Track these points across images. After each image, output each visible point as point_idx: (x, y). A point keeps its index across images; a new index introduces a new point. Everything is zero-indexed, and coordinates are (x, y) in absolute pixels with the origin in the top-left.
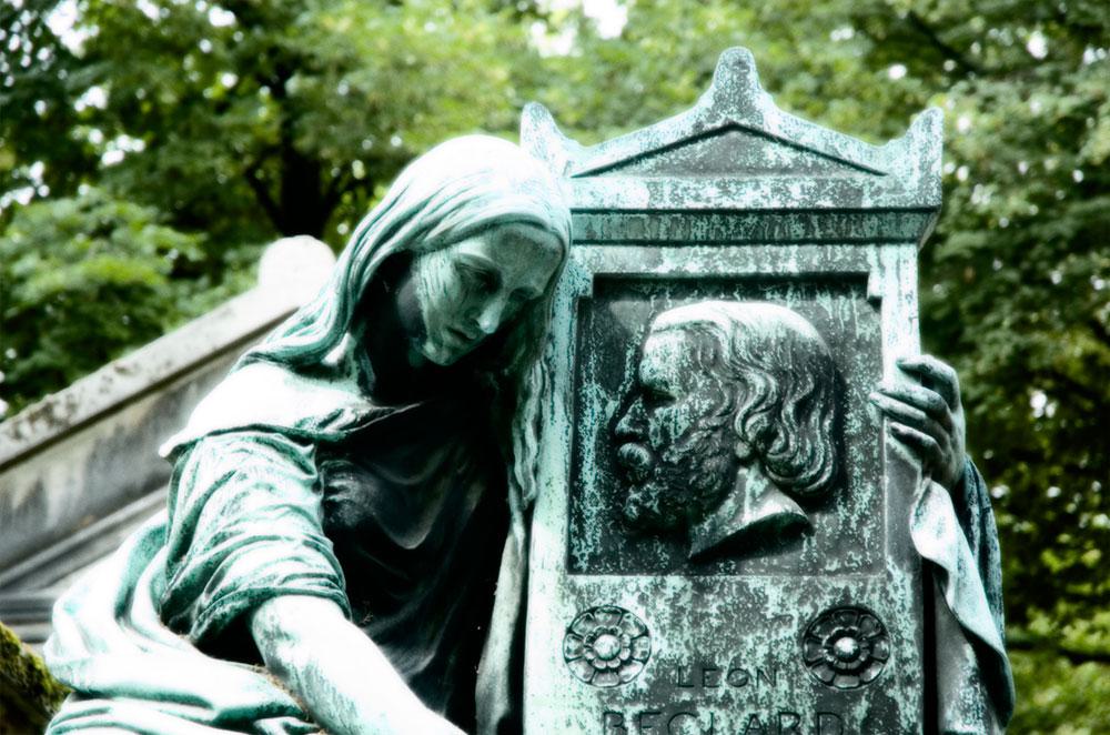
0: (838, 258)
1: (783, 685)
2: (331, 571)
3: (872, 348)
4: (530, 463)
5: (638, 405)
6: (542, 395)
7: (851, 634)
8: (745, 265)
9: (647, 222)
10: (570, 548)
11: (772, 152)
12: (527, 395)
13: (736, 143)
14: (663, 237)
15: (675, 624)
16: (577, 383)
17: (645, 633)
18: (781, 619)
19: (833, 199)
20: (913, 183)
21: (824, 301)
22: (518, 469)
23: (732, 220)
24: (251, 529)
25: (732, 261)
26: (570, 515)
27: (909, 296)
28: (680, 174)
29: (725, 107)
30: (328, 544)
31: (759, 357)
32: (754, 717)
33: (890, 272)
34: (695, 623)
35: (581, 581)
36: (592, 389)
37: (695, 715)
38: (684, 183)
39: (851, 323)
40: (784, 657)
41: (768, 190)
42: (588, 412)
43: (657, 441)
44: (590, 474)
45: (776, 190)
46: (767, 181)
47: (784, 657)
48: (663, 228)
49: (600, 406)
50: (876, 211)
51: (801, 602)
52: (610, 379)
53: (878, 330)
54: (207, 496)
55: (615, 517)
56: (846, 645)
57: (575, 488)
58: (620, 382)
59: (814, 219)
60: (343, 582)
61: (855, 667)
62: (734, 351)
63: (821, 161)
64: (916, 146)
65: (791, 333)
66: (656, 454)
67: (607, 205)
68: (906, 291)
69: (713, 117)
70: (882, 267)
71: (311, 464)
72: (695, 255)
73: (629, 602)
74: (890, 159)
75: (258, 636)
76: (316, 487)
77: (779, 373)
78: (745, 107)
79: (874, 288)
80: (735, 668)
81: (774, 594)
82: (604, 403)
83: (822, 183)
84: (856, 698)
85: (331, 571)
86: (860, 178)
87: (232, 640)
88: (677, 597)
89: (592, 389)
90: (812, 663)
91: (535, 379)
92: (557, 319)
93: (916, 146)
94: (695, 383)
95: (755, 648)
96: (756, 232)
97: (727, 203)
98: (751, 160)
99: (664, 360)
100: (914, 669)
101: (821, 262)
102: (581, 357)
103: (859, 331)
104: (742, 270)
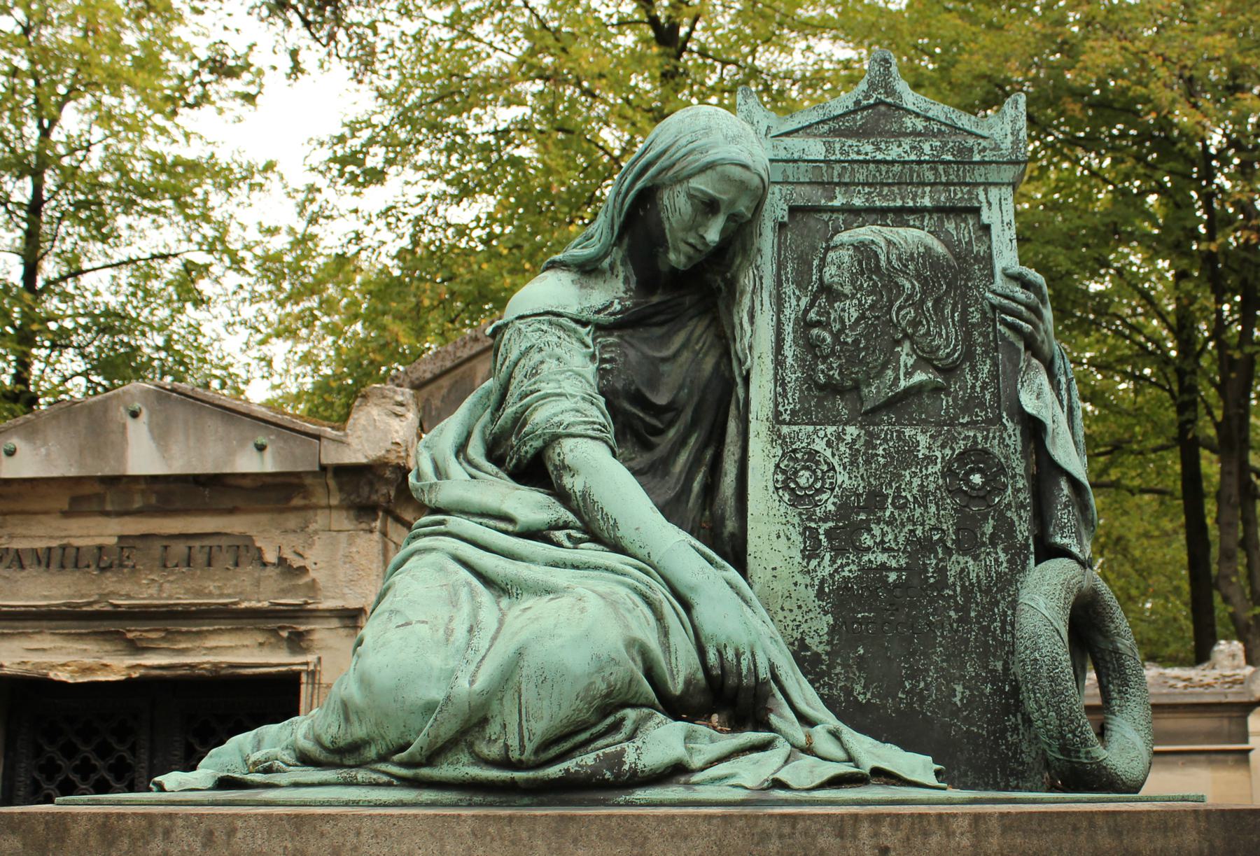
0: (959, 195)
2: (602, 420)
3: (988, 260)
4: (746, 341)
5: (823, 300)
6: (753, 292)
7: (980, 471)
8: (894, 200)
9: (824, 169)
10: (776, 405)
11: (909, 122)
12: (742, 293)
13: (884, 114)
14: (836, 180)
15: (853, 462)
16: (779, 283)
17: (833, 469)
18: (931, 460)
19: (954, 155)
21: (950, 226)
22: (738, 345)
23: (884, 168)
24: (547, 388)
25: (885, 197)
26: (776, 381)
27: (1009, 224)
28: (847, 137)
29: (875, 90)
30: (601, 401)
31: (906, 266)
32: (913, 531)
33: (995, 207)
35: (785, 430)
36: (789, 289)
37: (869, 530)
38: (850, 142)
39: (969, 243)
41: (907, 148)
42: (787, 305)
43: (836, 327)
44: (789, 351)
45: (913, 148)
46: (907, 143)
47: (932, 487)
48: (836, 173)
49: (795, 303)
50: (982, 163)
51: (943, 446)
52: (801, 284)
53: (990, 247)
54: (516, 364)
55: (809, 380)
56: (977, 479)
57: (779, 362)
58: (809, 284)
59: (941, 168)
60: (612, 429)
61: (983, 496)
62: (889, 262)
63: (943, 128)
64: (1008, 119)
65: (928, 249)
66: (836, 336)
67: (796, 156)
68: (1006, 220)
69: (867, 97)
70: (989, 204)
71: (589, 340)
72: (859, 192)
73: (819, 445)
74: (991, 127)
75: (551, 468)
76: (593, 357)
77: (918, 276)
78: (891, 91)
79: (985, 218)
80: (897, 496)
81: (923, 440)
82: (799, 299)
83: (945, 144)
84: (985, 519)
85: (602, 420)
86: (971, 141)
87: (535, 471)
88: (854, 441)
89: (789, 289)
90: (953, 492)
91: (747, 281)
92: (764, 237)
93: (1008, 119)
94: (862, 284)
95: (912, 482)
96: (900, 177)
97: (880, 156)
98: (895, 127)
99: (839, 267)
101: (947, 199)
102: (780, 266)
103: (975, 249)
104: (892, 204)
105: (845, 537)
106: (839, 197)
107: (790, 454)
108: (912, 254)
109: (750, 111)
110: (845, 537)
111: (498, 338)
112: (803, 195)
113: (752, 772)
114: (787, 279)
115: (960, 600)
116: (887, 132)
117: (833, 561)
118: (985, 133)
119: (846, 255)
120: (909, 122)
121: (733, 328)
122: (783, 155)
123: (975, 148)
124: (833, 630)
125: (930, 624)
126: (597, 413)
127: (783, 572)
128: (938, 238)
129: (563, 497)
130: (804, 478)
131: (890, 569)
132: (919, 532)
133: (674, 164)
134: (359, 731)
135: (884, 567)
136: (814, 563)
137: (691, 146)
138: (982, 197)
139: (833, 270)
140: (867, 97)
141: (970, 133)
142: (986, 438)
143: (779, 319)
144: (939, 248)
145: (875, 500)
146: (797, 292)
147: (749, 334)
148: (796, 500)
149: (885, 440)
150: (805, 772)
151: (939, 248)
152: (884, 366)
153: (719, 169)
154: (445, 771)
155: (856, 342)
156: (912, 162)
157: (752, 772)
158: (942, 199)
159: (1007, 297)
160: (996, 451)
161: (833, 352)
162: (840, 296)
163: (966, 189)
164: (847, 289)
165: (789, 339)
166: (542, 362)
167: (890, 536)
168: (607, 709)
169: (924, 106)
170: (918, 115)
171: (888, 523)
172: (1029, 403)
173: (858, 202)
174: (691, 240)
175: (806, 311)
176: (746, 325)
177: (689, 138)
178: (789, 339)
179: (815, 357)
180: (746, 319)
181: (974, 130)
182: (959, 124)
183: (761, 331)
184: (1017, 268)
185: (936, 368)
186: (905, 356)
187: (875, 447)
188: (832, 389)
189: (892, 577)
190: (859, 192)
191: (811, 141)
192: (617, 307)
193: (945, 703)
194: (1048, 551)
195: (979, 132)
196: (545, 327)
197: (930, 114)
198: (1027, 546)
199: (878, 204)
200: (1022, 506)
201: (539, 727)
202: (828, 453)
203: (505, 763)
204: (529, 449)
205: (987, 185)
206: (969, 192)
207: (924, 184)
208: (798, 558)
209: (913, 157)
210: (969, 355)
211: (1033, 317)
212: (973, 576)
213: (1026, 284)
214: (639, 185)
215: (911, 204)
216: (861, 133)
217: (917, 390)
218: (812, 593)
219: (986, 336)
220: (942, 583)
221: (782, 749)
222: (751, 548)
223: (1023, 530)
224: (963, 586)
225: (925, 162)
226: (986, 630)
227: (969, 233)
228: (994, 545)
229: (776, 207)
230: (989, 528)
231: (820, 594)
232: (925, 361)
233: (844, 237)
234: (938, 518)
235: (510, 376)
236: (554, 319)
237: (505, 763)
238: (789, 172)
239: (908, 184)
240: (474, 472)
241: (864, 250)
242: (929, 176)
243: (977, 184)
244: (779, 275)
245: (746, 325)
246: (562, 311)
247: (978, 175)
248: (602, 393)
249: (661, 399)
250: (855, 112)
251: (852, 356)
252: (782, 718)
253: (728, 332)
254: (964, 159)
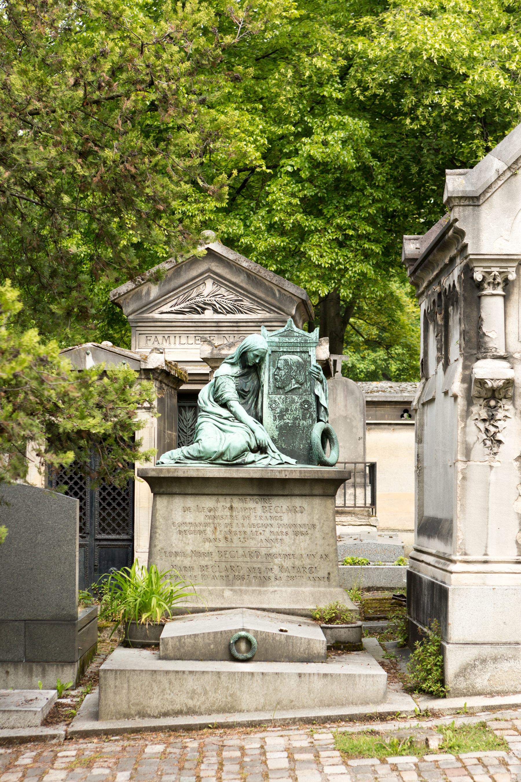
3: (310, 362)
44: (271, 380)
49: (272, 370)
52: (274, 366)
55: (275, 386)
61: (307, 409)
87: (225, 405)
91: (263, 367)
95: (294, 406)
105: (281, 417)
107: (271, 401)
110: (281, 417)
112: (274, 348)
113: (265, 462)
119: (282, 361)
120: (295, 334)
126: (236, 396)
129: (231, 411)
130: (274, 405)
134: (202, 455)
144: (301, 360)
148: (272, 410)
150: (274, 462)
151: (301, 360)
154: (217, 462)
157: (265, 462)
168: (243, 452)
172: (317, 392)
183: (266, 376)
186: (293, 381)
188: (279, 388)
193: (299, 448)
194: (319, 420)
201: (233, 454)
203: (227, 461)
204: (224, 402)
210: (306, 381)
213: (317, 368)
216: (286, 336)
217: (296, 388)
221: (270, 458)
223: (315, 416)
229: (269, 352)
232: (297, 382)
233: (281, 358)
234: (299, 413)
237: (227, 461)
241: (286, 361)
249: (247, 390)
251: (283, 382)
252: (269, 451)
254: (306, 342)
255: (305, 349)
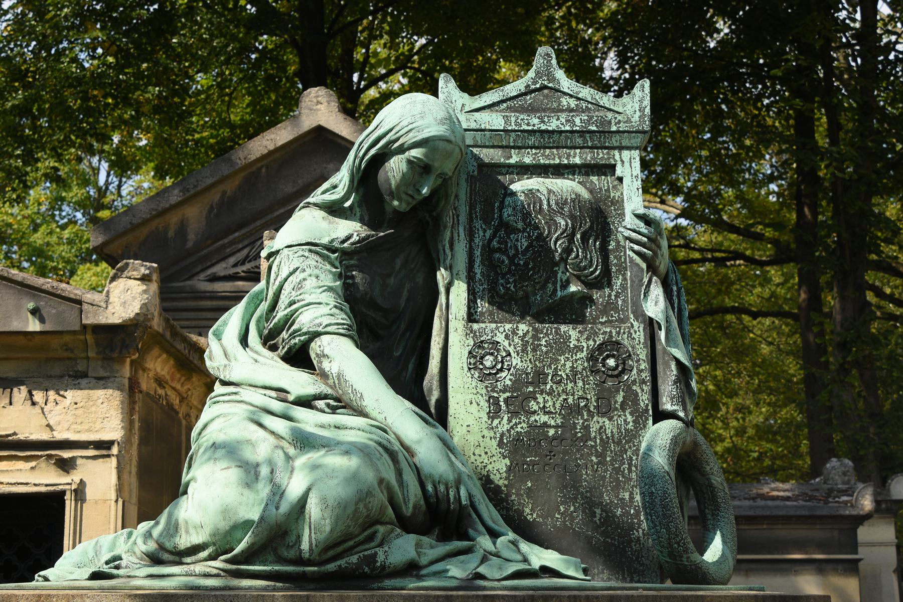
1: (580, 384)
5: (502, 233)
6: (452, 227)
8: (554, 159)
11: (565, 101)
12: (445, 227)
14: (512, 144)
15: (524, 350)
16: (470, 220)
17: (509, 354)
18: (579, 349)
20: (636, 117)
21: (594, 179)
24: (309, 299)
25: (547, 157)
27: (637, 177)
28: (519, 112)
29: (541, 78)
31: (562, 209)
32: (565, 400)
33: (627, 164)
34: (534, 350)
35: (475, 326)
36: (478, 224)
37: (535, 399)
38: (522, 117)
39: (608, 190)
40: (580, 368)
41: (564, 121)
42: (477, 235)
43: (512, 252)
44: (478, 270)
46: (563, 117)
47: (580, 368)
48: (512, 140)
50: (618, 132)
51: (588, 339)
52: (487, 220)
54: (286, 280)
56: (611, 362)
58: (492, 220)
60: (355, 327)
63: (590, 106)
66: (512, 259)
68: (635, 174)
69: (535, 83)
71: (337, 264)
72: (528, 153)
73: (500, 338)
74: (624, 105)
77: (572, 217)
78: (552, 78)
81: (574, 334)
82: (485, 231)
83: (591, 118)
86: (610, 115)
87: (300, 357)
88: (525, 335)
89: (478, 224)
90: (594, 371)
95: (565, 365)
97: (543, 127)
99: (514, 209)
100: (646, 375)
101: (592, 158)
102: (472, 207)
103: (612, 195)
104: (552, 162)
105: (518, 403)
106: (514, 156)
108: (566, 199)
109: (450, 93)
110: (518, 403)
111: (271, 260)
114: (477, 217)
115: (599, 449)
116: (550, 108)
117: (509, 421)
118: (620, 110)
121: (438, 252)
122: (473, 126)
123: (613, 121)
124: (509, 469)
125: (578, 466)
127: (475, 428)
128: (585, 187)
130: (489, 361)
131: (550, 426)
132: (570, 401)
133: (398, 139)
135: (545, 425)
136: (496, 422)
137: (410, 127)
138: (617, 157)
139: (510, 211)
140: (535, 83)
141: (610, 110)
142: (618, 333)
143: (471, 246)
145: (539, 377)
146: (484, 226)
147: (449, 258)
149: (547, 334)
151: (585, 194)
152: (547, 282)
153: (431, 143)
155: (526, 264)
156: (567, 131)
158: (589, 158)
159: (634, 231)
160: (626, 342)
161: (509, 272)
162: (516, 231)
163: (605, 151)
164: (520, 225)
165: (478, 261)
166: (304, 279)
167: (550, 403)
169: (576, 89)
170: (571, 96)
171: (549, 394)
173: (527, 160)
174: (410, 193)
175: (490, 240)
176: (448, 251)
177: (409, 120)
178: (478, 261)
179: (497, 274)
180: (447, 245)
181: (612, 107)
182: (601, 103)
184: (641, 211)
185: (583, 282)
187: (539, 339)
189: (552, 432)
190: (528, 153)
191: (494, 115)
192: (355, 238)
194: (660, 416)
195: (616, 109)
196: (307, 254)
197: (580, 96)
198: (647, 411)
199: (542, 161)
200: (643, 382)
202: (506, 343)
205: (621, 148)
206: (608, 153)
207: (575, 148)
208: (485, 418)
209: (568, 128)
211: (653, 246)
212: (608, 431)
214: (373, 152)
215: (566, 162)
216: (531, 110)
218: (494, 443)
219: (618, 258)
220: (586, 437)
222: (451, 411)
223: (644, 399)
224: (601, 439)
225: (576, 131)
226: (618, 471)
227: (608, 183)
228: (624, 410)
230: (620, 398)
231: (501, 444)
234: (583, 390)
235: (281, 288)
236: (313, 248)
238: (478, 139)
239: (564, 148)
240: (255, 356)
242: (579, 141)
243: (614, 148)
244: (470, 214)
245: (448, 251)
246: (318, 242)
247: (615, 141)
248: (346, 301)
250: (525, 94)
253: (434, 255)
255: (601, 155)
